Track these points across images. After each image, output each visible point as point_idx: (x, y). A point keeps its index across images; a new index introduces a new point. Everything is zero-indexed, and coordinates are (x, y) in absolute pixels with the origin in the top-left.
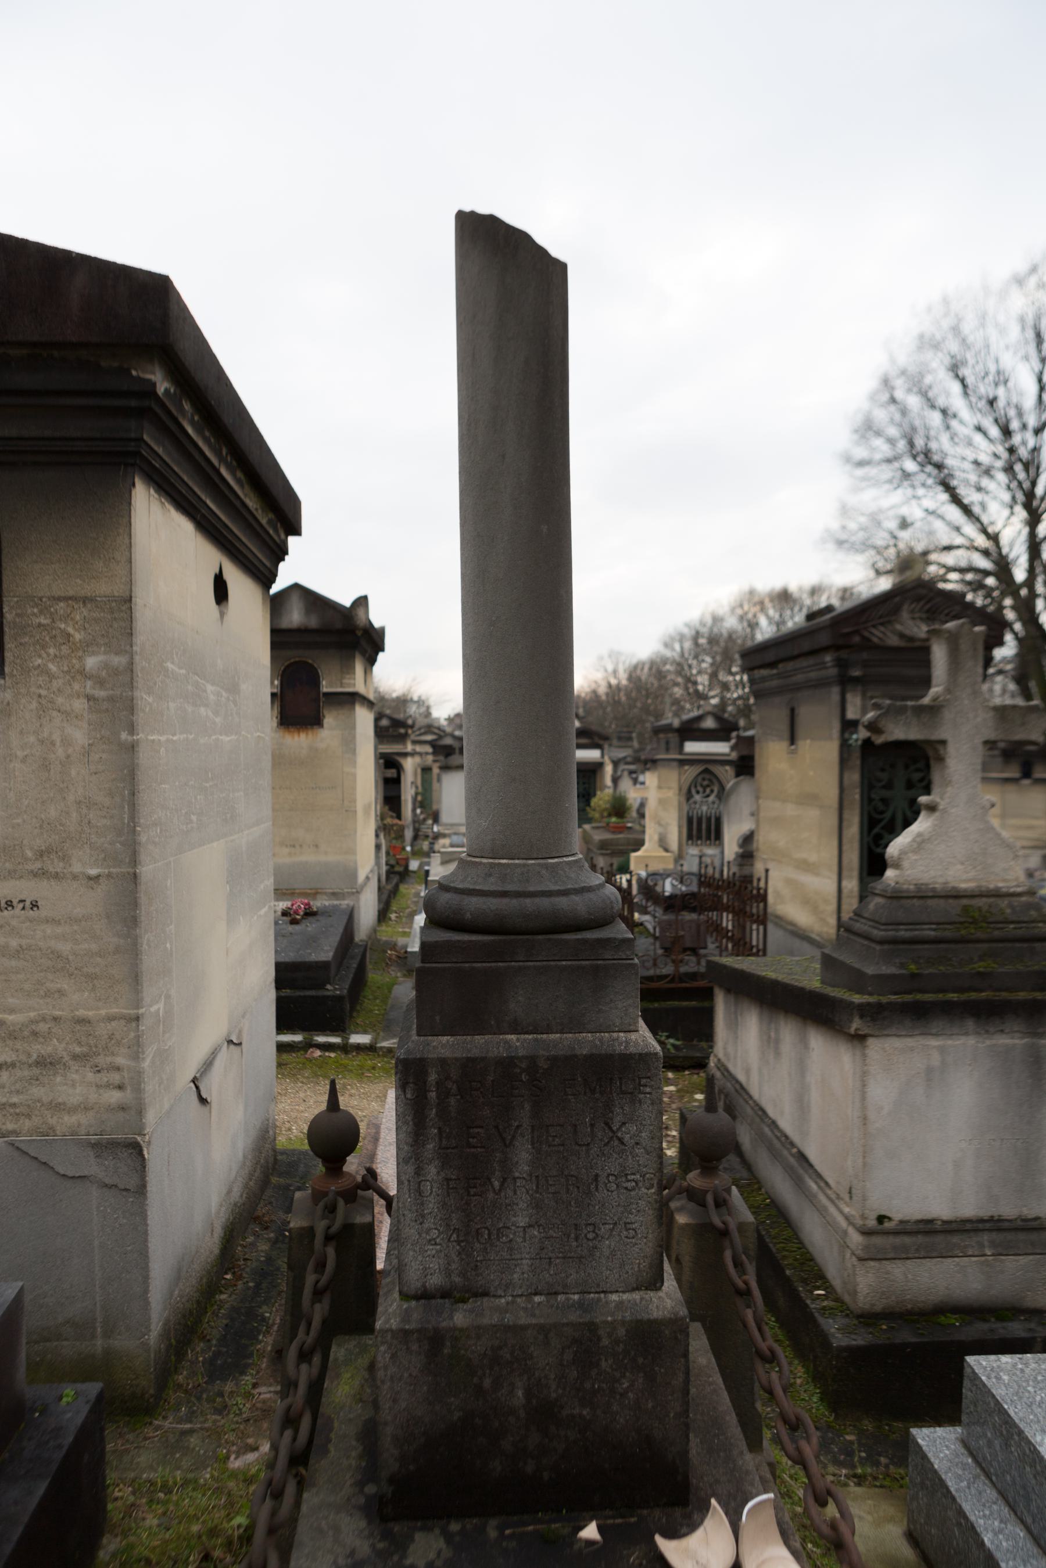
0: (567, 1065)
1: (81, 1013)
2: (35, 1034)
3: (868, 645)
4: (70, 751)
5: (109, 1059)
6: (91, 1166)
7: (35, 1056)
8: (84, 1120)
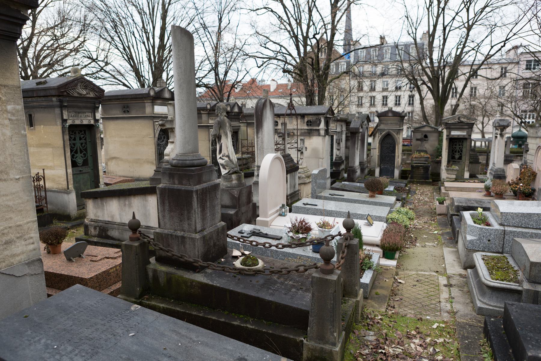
0: (212, 186)
1: (18, 223)
2: (3, 234)
3: (68, 95)
4: (5, 137)
5: (29, 236)
6: (27, 270)
7: (4, 241)
8: (23, 257)
